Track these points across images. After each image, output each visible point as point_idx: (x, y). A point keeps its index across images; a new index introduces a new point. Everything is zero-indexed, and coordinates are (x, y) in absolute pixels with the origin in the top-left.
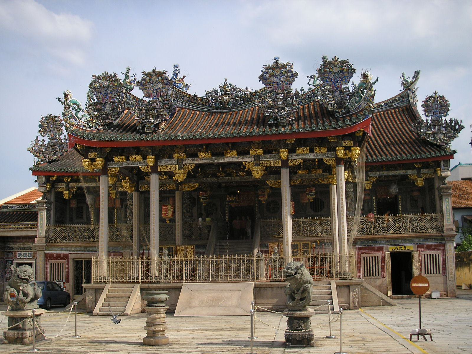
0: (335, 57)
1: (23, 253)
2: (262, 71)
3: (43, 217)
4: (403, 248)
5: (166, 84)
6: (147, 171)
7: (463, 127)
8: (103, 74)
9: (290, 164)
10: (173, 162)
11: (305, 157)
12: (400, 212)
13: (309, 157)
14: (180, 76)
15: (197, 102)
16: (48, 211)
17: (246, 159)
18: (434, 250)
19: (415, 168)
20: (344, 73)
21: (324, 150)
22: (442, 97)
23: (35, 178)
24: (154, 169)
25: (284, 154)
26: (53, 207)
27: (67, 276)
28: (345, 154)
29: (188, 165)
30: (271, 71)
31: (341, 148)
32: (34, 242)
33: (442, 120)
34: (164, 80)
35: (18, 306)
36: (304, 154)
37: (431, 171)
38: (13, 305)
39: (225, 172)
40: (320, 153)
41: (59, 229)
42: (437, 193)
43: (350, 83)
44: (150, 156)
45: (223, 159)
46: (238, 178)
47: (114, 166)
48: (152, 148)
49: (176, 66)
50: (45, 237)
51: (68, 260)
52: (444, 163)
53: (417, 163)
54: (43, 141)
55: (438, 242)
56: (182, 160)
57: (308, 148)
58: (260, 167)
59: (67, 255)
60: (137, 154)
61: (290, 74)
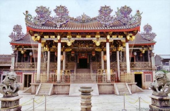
3: (13, 59)
4: (139, 72)
5: (65, 11)
6: (57, 42)
7: (156, 35)
9: (110, 41)
16: (15, 57)
18: (149, 74)
19: (142, 47)
21: (122, 37)
22: (150, 26)
23: (11, 46)
24: (59, 41)
25: (108, 37)
26: (17, 56)
27: (22, 81)
30: (103, 9)
32: (10, 68)
35: (8, 95)
36: (115, 38)
37: (147, 48)
38: (4, 94)
39: (81, 45)
40: (121, 38)
42: (149, 55)
43: (130, 15)
46: (85, 48)
51: (22, 75)
53: (142, 45)
54: (14, 34)
55: (150, 71)
56: (70, 38)
57: (116, 36)
59: (22, 73)
60: (53, 35)
61: (110, 10)
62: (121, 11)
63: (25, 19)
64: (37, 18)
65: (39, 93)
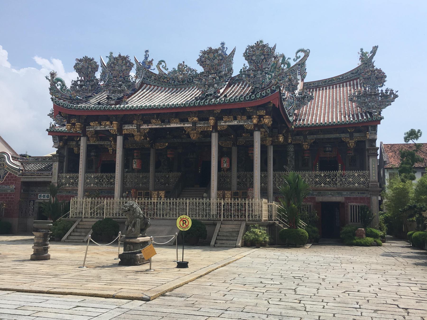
1: (42, 195)
5: (129, 67)
6: (114, 133)
7: (396, 96)
8: (84, 57)
10: (134, 127)
11: (230, 124)
12: (340, 169)
13: (233, 124)
14: (149, 59)
15: (161, 80)
17: (186, 125)
20: (264, 55)
21: (245, 118)
25: (212, 122)
28: (259, 121)
29: (144, 129)
30: (206, 55)
31: (254, 116)
33: (378, 90)
34: (127, 63)
41: (68, 177)
44: (114, 122)
45: (170, 125)
47: (91, 129)
48: (116, 116)
49: (147, 51)
50: (57, 183)
52: (372, 128)
58: (195, 132)
61: (220, 57)
62: (248, 56)
63: (50, 89)
64: (79, 83)
65: (71, 237)
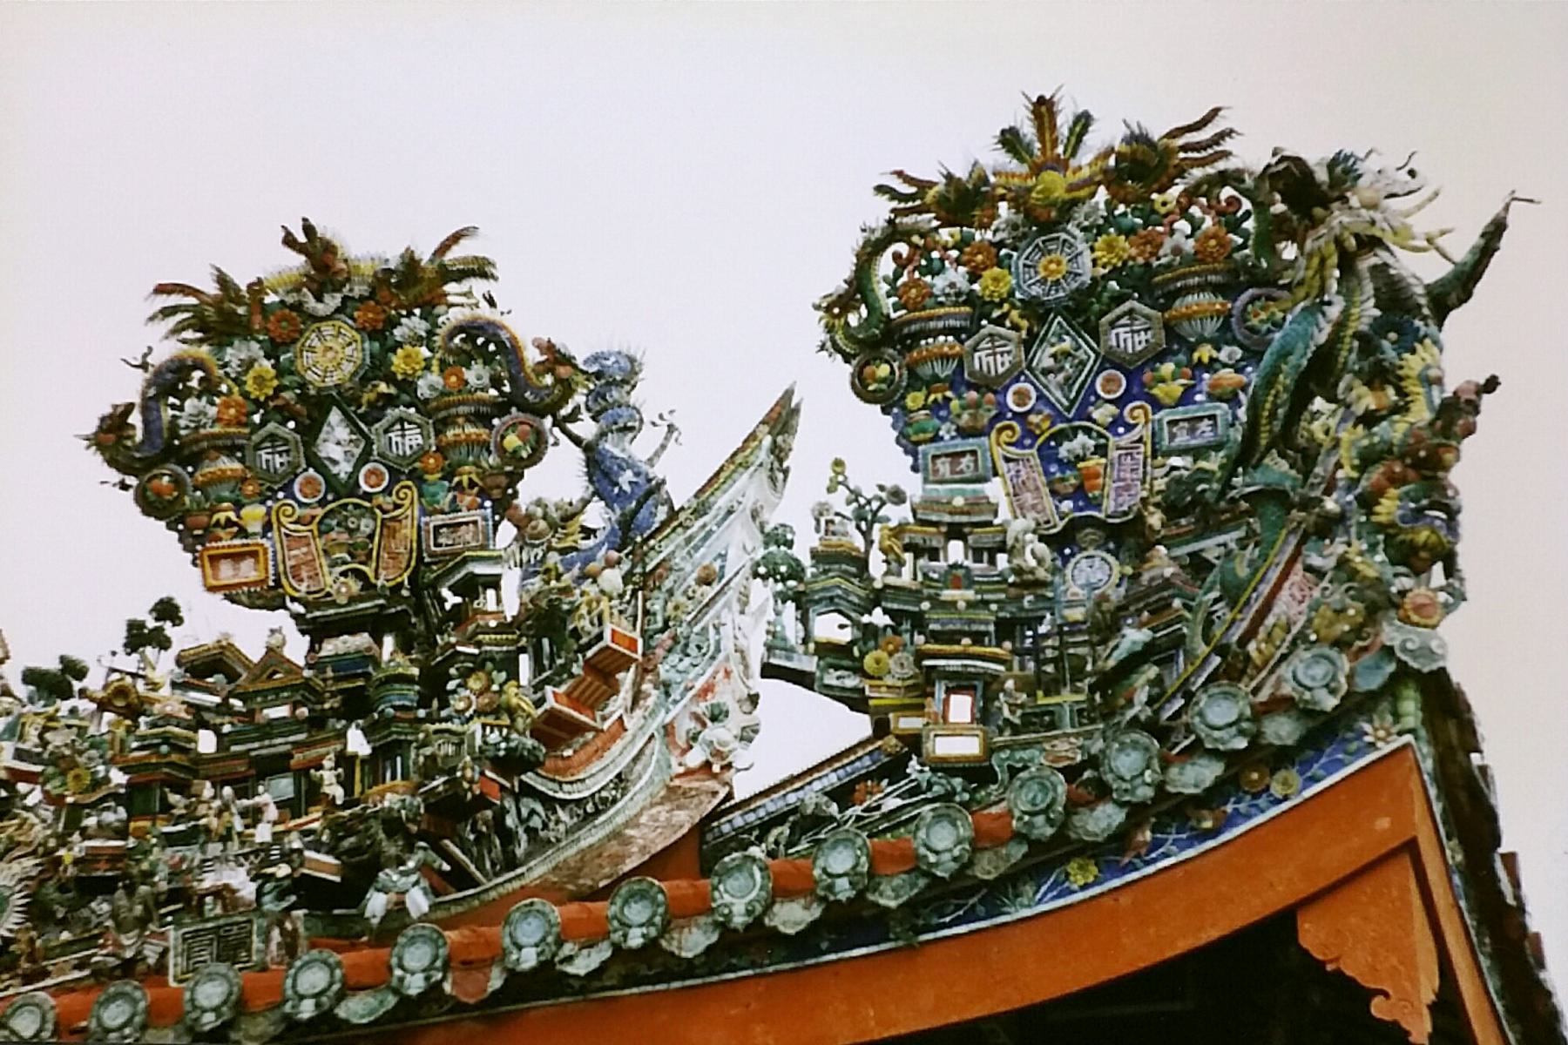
0: (1043, 109)
2: (144, 366)
